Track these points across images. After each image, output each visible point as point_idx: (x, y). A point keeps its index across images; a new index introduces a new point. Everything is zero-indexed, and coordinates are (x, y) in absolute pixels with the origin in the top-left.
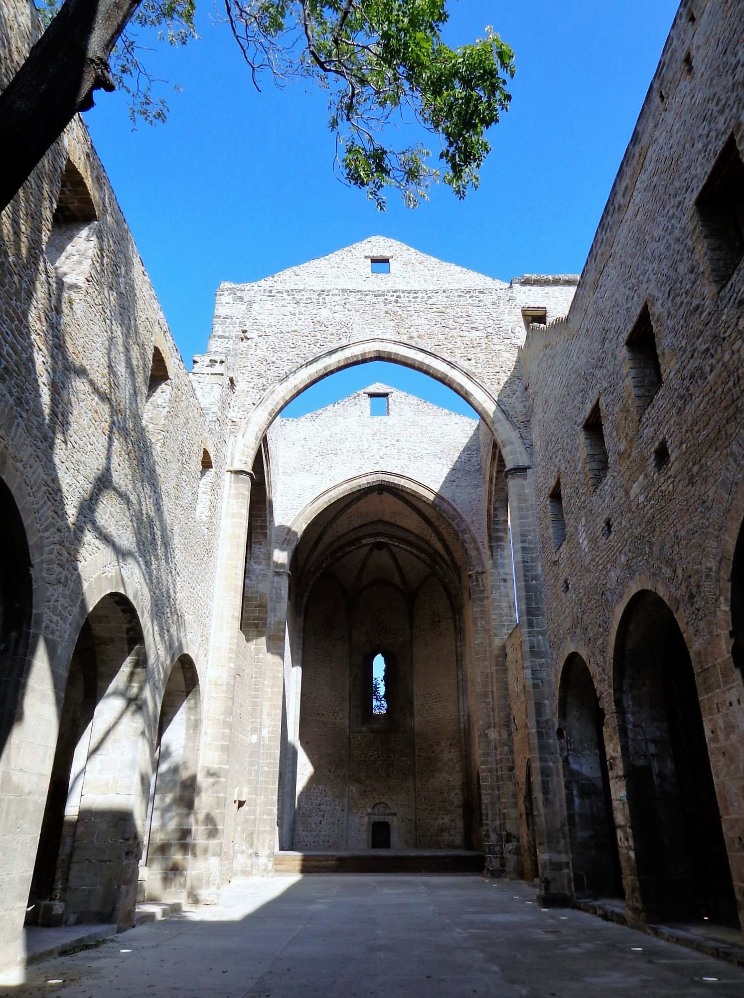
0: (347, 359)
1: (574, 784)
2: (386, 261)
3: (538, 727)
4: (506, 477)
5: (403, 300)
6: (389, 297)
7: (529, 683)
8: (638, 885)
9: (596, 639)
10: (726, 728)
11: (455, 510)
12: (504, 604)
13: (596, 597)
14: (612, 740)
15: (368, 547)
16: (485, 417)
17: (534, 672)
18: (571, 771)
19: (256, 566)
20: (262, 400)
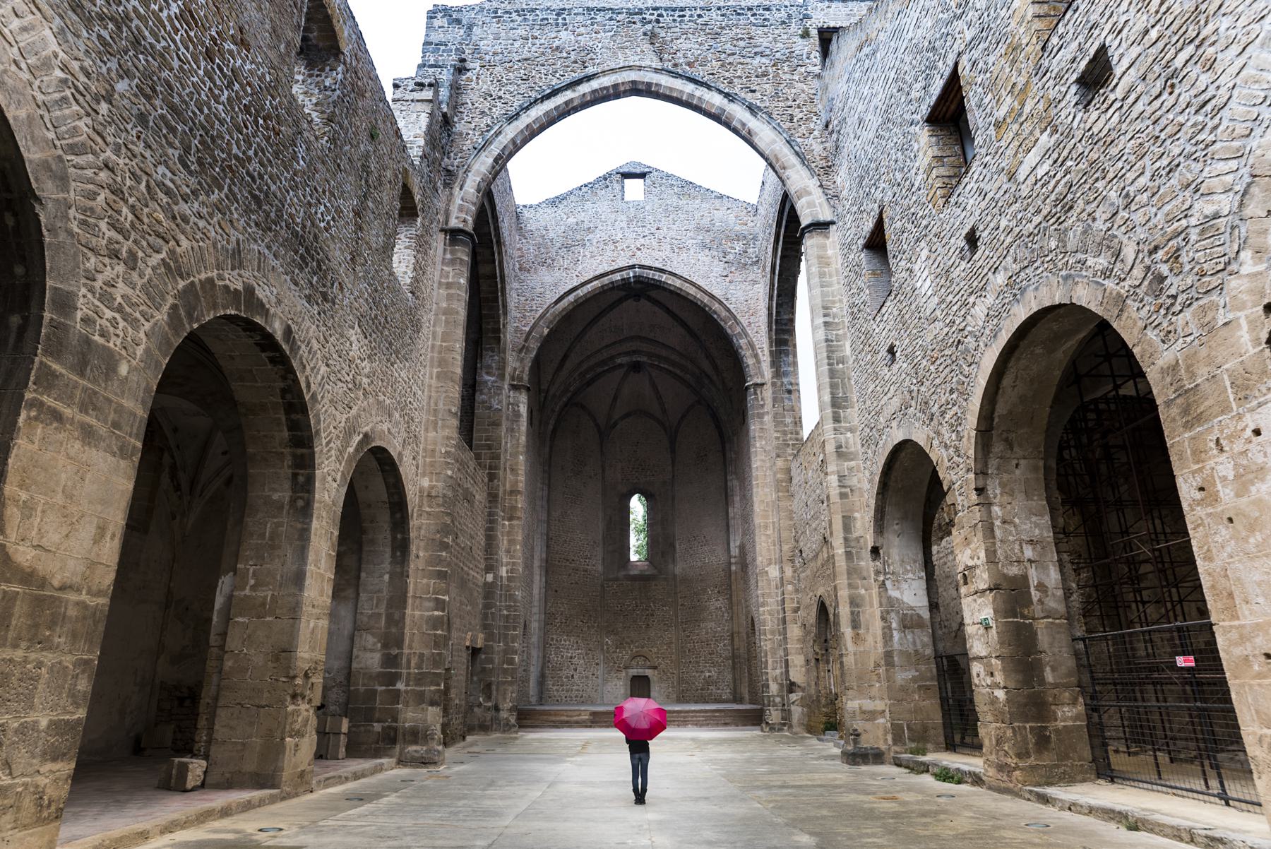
0: (594, 92)
1: (893, 615)
4: (802, 236)
5: (667, 19)
6: (647, 16)
7: (834, 493)
8: (1009, 733)
9: (943, 414)
10: (1238, 477)
11: (728, 310)
12: (788, 420)
13: (947, 352)
14: (968, 544)
15: (622, 371)
16: (774, 162)
17: (841, 478)
18: (889, 598)
19: (487, 378)
20: (488, 143)
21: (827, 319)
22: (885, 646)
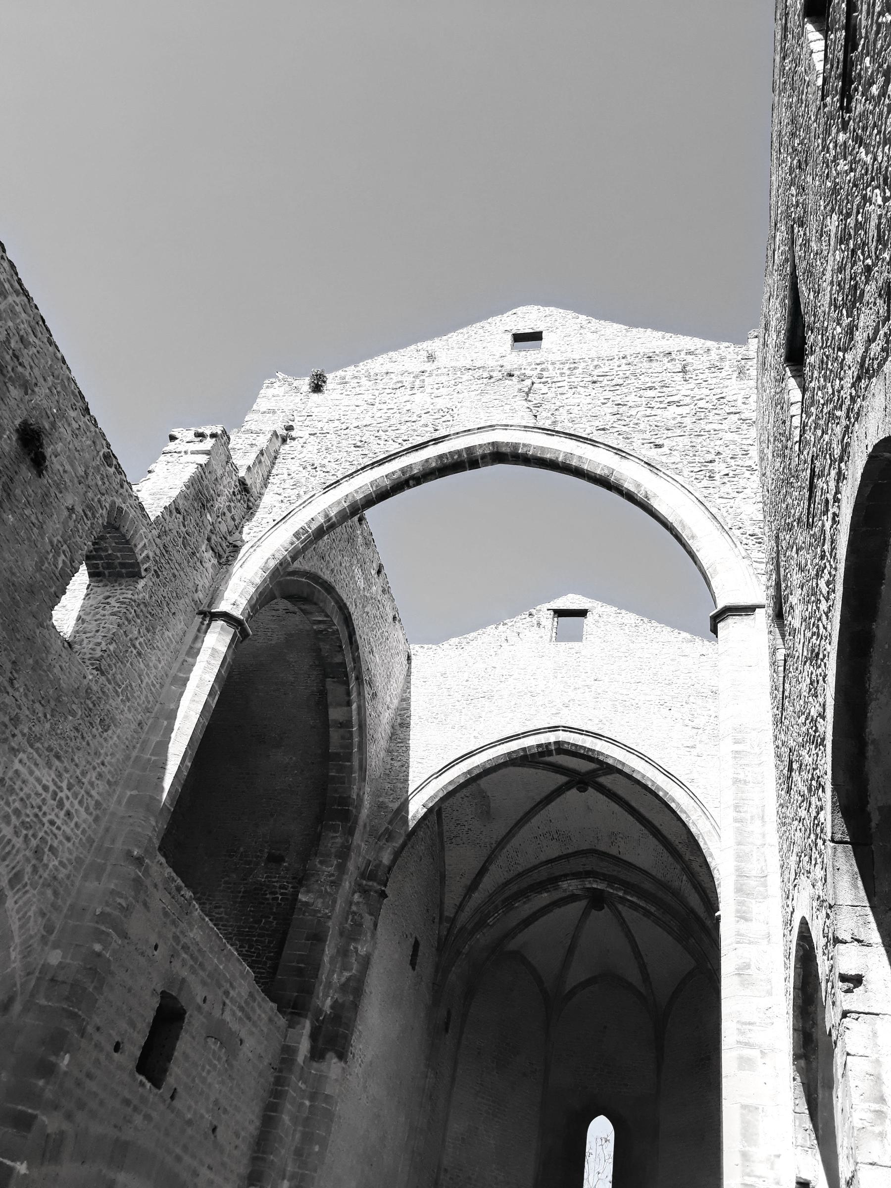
2: (536, 336)
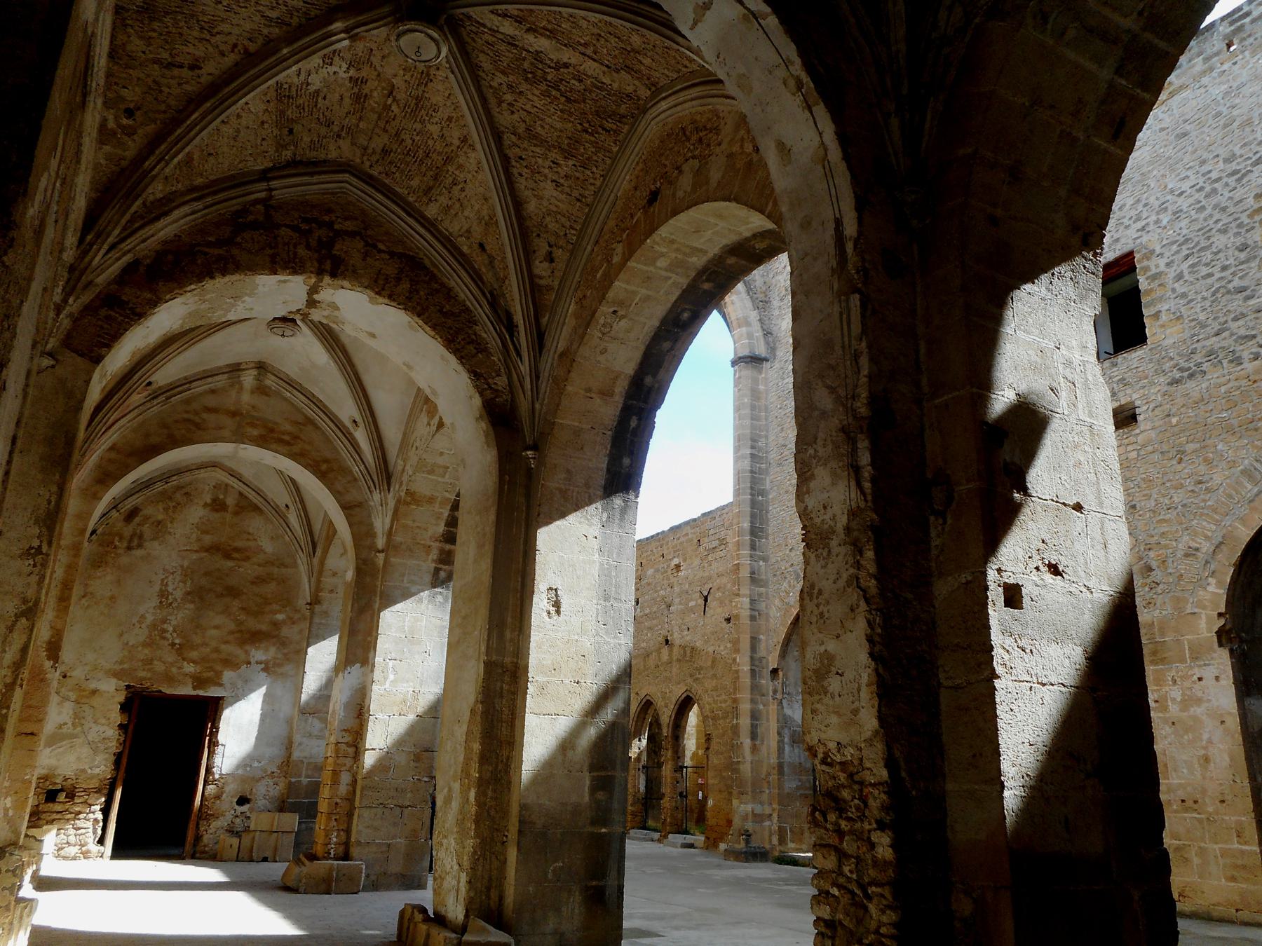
1: (786, 731)
3: (752, 665)
17: (753, 602)
21: (754, 452)
22: (778, 758)
